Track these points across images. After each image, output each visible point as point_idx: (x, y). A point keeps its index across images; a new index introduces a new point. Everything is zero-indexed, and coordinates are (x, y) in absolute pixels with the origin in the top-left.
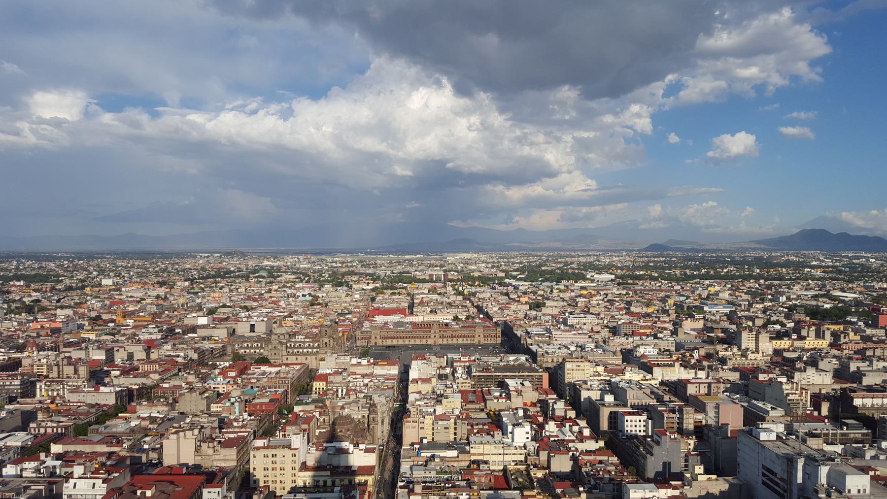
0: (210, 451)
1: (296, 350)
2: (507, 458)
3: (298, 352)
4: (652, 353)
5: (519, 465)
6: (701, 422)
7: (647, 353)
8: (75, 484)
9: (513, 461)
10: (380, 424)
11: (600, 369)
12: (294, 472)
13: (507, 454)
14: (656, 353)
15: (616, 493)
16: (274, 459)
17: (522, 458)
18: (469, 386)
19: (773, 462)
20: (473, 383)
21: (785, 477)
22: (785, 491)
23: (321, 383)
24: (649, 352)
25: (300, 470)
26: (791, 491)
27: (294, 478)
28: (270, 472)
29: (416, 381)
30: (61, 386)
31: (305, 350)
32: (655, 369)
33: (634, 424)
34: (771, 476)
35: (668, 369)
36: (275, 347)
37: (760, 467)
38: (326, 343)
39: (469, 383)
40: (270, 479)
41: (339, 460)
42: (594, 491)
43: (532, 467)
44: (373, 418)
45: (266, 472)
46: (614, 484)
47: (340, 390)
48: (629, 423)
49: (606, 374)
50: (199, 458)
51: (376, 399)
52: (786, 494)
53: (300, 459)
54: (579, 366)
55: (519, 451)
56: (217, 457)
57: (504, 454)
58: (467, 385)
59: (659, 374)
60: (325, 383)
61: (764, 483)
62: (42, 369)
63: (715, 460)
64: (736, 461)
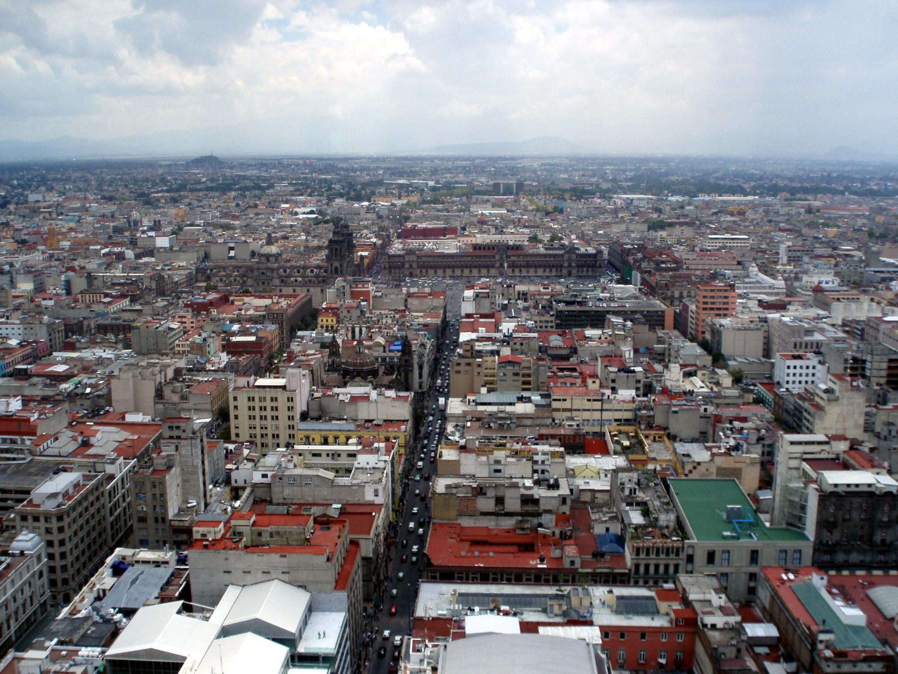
0: (175, 398)
1: (292, 279)
2: (607, 415)
3: (296, 281)
4: (830, 285)
5: (624, 425)
7: (823, 285)
9: (616, 420)
10: (416, 372)
11: (753, 305)
12: (291, 423)
13: (606, 410)
14: (836, 284)
15: (766, 458)
17: (628, 415)
18: (552, 327)
20: (558, 322)
23: (330, 320)
24: (827, 283)
27: (292, 432)
28: (258, 422)
29: (469, 316)
32: (835, 305)
35: (853, 306)
36: (263, 273)
38: (336, 268)
39: (552, 322)
40: (258, 431)
41: (356, 411)
42: (733, 453)
43: (643, 427)
44: (406, 361)
45: (252, 422)
46: (764, 446)
47: (357, 330)
48: (792, 371)
49: (761, 310)
50: (160, 406)
51: (411, 335)
53: (301, 405)
55: (626, 406)
56: (186, 406)
57: (602, 410)
58: (550, 324)
59: (840, 312)
60: (335, 319)
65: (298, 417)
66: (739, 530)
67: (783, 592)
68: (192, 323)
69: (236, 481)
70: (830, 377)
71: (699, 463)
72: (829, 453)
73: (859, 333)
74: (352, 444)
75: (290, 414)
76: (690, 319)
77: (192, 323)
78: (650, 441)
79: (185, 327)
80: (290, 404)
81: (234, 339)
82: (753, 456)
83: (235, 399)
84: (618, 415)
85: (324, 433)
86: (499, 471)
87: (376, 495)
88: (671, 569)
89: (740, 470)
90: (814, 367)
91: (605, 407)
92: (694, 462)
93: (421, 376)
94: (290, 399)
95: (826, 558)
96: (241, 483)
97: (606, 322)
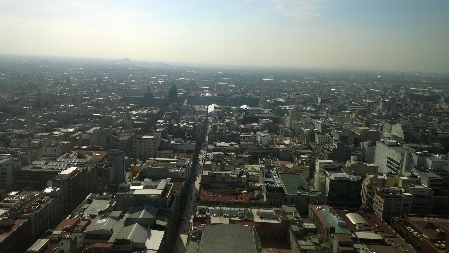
2: (259, 151)
4: (335, 111)
6: (358, 139)
8: (46, 149)
9: (262, 153)
13: (259, 150)
16: (145, 144)
17: (265, 151)
19: (394, 155)
21: (399, 162)
22: (398, 168)
24: (334, 110)
25: (158, 150)
26: (402, 169)
30: (39, 111)
31: (161, 103)
33: (323, 139)
34: (392, 162)
37: (387, 158)
42: (300, 165)
47: (178, 120)
49: (311, 118)
52: (398, 170)
54: (297, 114)
57: (257, 149)
61: (388, 166)
62: (28, 104)
63: (363, 157)
64: (374, 156)
65: (157, 148)
66: (302, 191)
67: (317, 213)
68: (121, 116)
69: (135, 170)
70: (334, 141)
71: (289, 168)
72: (333, 167)
73: (345, 127)
74: (175, 158)
75: (155, 148)
76: (287, 121)
77: (121, 116)
78: (273, 160)
79: (118, 117)
80: (155, 144)
81: (135, 122)
82: (307, 167)
83: (135, 142)
84: (262, 151)
85: (166, 154)
86: (224, 168)
87: (183, 175)
88: (279, 203)
89: (303, 171)
90: (328, 138)
91: (258, 148)
92: (287, 167)
93: (199, 137)
94: (155, 143)
95: (332, 202)
96: (136, 171)
97: (259, 121)
